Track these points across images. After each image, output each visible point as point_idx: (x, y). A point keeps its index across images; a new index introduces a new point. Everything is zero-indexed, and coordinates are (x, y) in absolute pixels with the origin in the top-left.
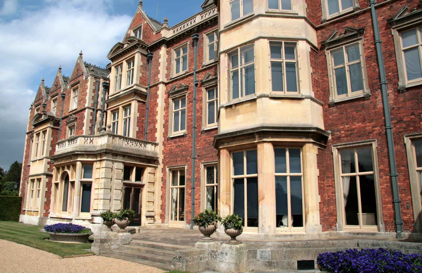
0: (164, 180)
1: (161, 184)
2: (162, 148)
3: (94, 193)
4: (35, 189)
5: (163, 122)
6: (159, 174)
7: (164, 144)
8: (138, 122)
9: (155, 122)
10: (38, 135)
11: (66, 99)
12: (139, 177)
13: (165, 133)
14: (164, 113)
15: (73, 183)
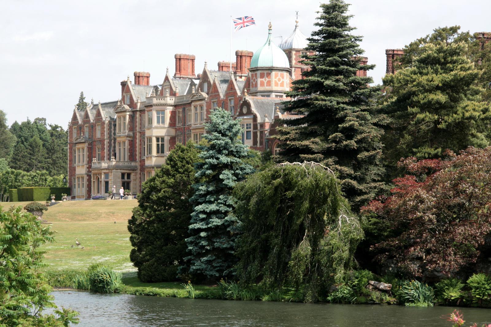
0: (140, 178)
1: (140, 180)
2: (140, 163)
3: (110, 185)
4: (80, 183)
5: (140, 151)
6: (138, 176)
7: (140, 162)
8: (129, 151)
9: (136, 151)
10: (79, 149)
11: (94, 129)
12: (129, 177)
13: (140, 157)
14: (140, 147)
15: (101, 181)
